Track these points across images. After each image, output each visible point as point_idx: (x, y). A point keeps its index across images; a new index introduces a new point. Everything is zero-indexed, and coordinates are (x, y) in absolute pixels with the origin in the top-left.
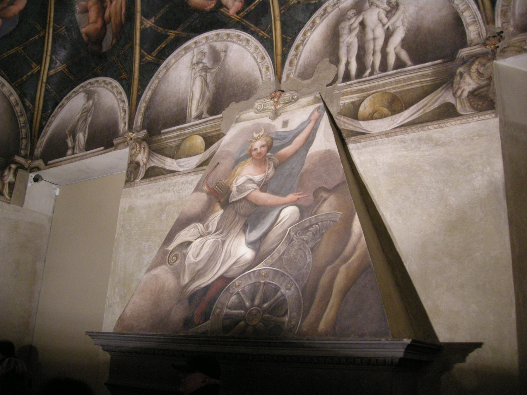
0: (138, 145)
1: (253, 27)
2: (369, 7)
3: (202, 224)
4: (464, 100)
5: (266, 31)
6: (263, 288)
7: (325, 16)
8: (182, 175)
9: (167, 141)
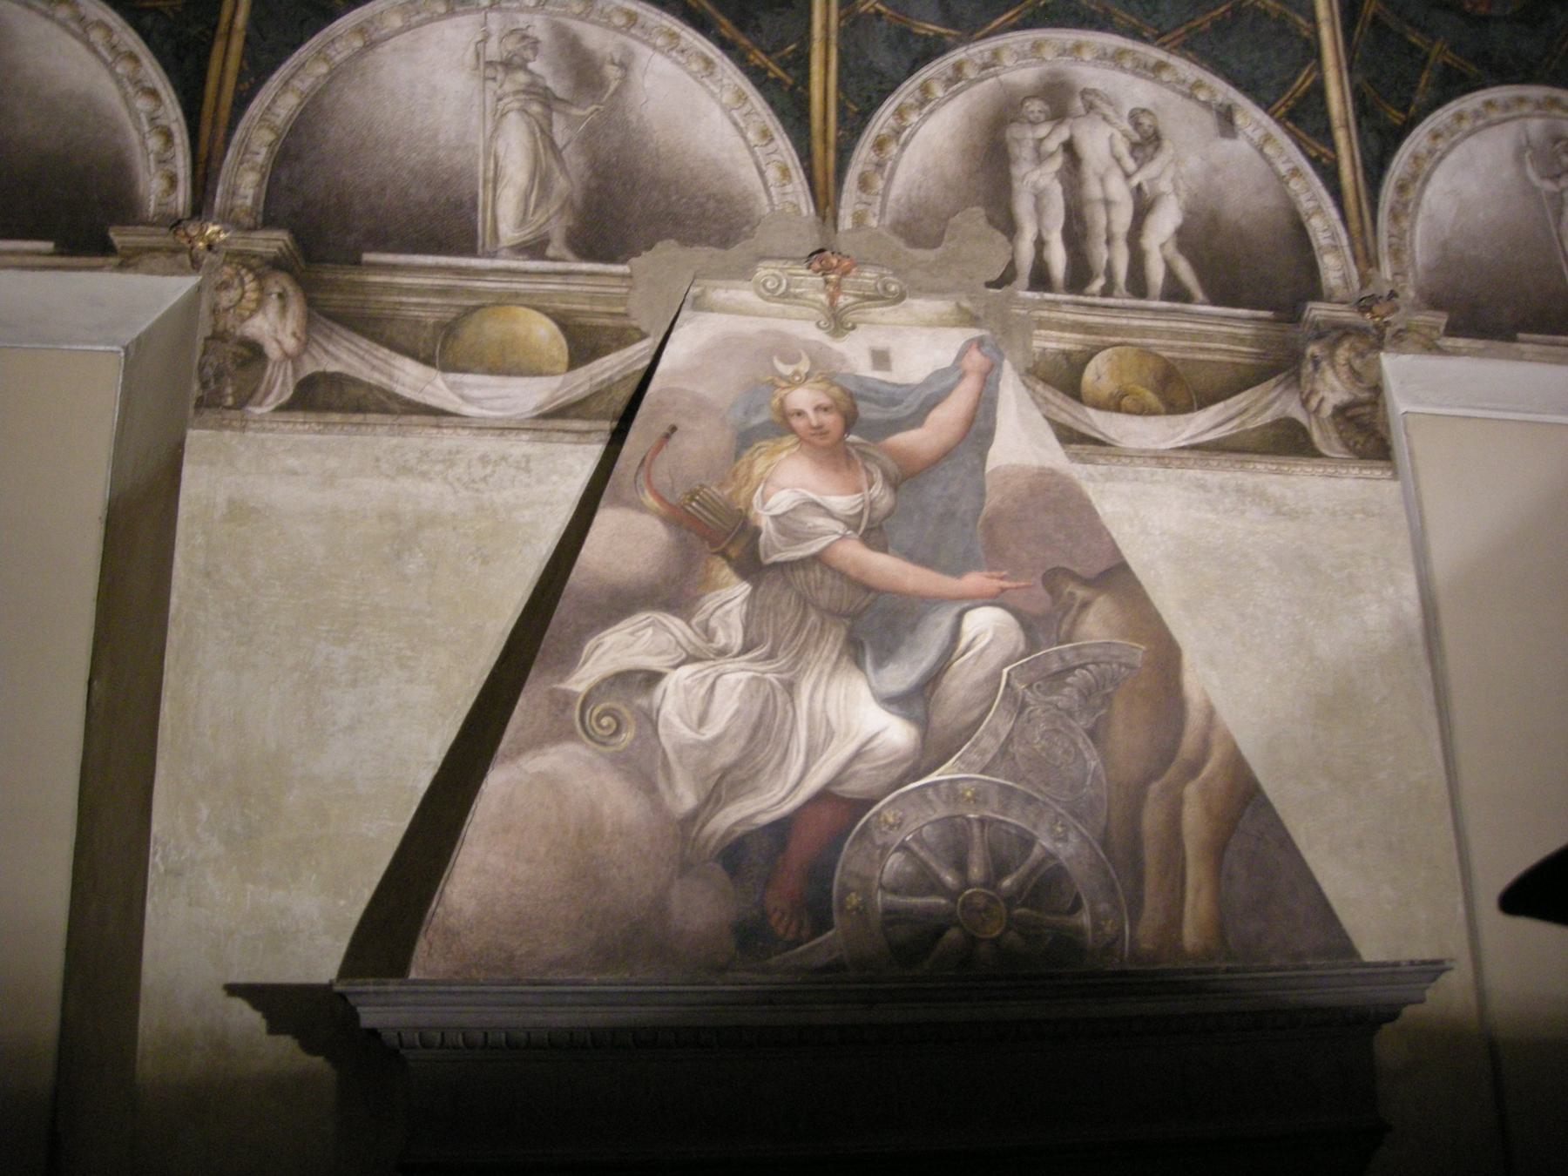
0: (249, 278)
1: (727, 28)
2: (1083, 112)
3: (681, 617)
4: (1326, 422)
5: (774, 57)
6: (982, 831)
7: (959, 85)
8: (475, 432)
9: (397, 299)
